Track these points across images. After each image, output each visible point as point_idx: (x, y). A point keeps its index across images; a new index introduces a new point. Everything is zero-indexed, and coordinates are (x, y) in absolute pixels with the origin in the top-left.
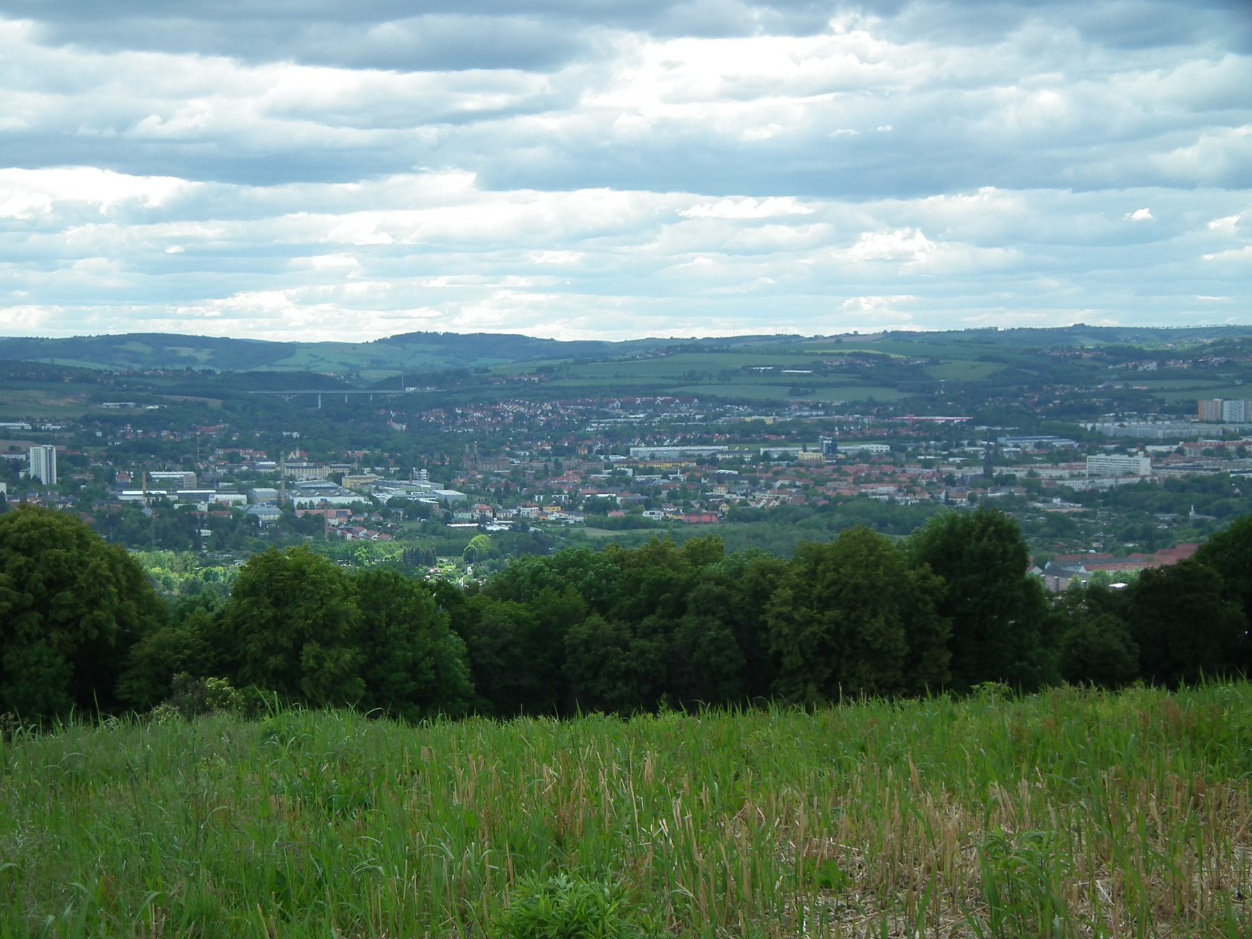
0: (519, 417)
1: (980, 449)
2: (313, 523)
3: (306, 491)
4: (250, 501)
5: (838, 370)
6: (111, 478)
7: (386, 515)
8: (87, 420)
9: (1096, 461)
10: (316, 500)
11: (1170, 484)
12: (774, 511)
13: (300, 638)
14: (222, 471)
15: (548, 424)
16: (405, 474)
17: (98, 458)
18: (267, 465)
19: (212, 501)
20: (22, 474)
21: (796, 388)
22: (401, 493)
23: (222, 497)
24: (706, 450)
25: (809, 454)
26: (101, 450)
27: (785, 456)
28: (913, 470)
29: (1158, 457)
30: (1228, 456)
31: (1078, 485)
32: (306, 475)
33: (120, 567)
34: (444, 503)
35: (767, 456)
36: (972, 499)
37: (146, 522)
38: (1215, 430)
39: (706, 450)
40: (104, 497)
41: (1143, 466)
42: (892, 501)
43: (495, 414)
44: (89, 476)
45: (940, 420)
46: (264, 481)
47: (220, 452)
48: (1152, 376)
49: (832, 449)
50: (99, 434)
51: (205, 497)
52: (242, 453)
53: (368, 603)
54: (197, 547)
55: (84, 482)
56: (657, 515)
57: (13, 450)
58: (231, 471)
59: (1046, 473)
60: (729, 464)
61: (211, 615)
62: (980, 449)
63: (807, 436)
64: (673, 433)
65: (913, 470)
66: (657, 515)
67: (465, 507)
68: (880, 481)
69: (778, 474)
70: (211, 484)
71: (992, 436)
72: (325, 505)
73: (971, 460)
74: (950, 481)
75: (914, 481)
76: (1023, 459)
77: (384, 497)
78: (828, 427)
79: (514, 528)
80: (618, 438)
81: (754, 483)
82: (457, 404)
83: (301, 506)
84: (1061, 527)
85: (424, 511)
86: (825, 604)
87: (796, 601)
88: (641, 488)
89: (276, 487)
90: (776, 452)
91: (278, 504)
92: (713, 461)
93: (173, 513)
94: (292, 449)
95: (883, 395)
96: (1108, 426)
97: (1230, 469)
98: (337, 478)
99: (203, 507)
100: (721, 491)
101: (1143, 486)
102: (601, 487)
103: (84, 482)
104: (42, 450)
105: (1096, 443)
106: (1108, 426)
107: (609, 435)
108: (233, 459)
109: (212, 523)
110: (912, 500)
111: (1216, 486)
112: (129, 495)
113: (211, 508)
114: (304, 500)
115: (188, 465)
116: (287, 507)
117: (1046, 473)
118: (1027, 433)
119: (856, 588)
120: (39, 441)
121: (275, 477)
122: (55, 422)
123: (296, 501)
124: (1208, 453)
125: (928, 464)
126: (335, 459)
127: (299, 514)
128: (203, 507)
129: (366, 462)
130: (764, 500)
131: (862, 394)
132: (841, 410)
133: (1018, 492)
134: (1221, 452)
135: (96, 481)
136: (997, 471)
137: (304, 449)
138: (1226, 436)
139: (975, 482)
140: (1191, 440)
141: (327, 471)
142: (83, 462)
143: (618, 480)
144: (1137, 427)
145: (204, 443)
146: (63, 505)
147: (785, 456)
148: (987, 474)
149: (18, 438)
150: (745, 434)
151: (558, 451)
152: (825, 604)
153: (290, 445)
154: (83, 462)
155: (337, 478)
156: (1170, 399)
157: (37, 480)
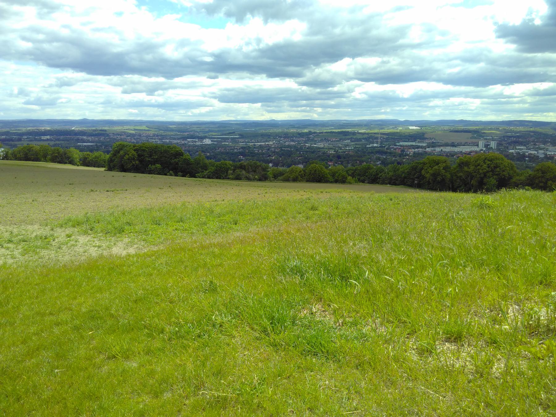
3: (550, 151)
4: (537, 153)
8: (504, 137)
14: (532, 147)
17: (505, 144)
19: (529, 153)
20: (489, 147)
23: (531, 152)
26: (505, 142)
32: (551, 148)
40: (506, 151)
44: (503, 147)
46: (541, 149)
47: (532, 143)
50: (506, 139)
51: (528, 152)
52: (537, 143)
54: (525, 161)
55: (502, 148)
57: (487, 142)
58: (534, 147)
61: (528, 175)
70: (530, 149)
83: (549, 154)
89: (544, 150)
91: (544, 154)
93: (520, 155)
94: (549, 143)
103: (502, 148)
104: (493, 142)
108: (535, 144)
112: (511, 151)
113: (529, 154)
114: (550, 153)
115: (525, 145)
116: (546, 155)
120: (493, 140)
122: (497, 137)
123: (548, 153)
127: (548, 156)
128: (527, 154)
135: (504, 148)
137: (551, 143)
142: (501, 145)
145: (529, 141)
146: (497, 154)
149: (489, 140)
153: (548, 142)
154: (501, 145)
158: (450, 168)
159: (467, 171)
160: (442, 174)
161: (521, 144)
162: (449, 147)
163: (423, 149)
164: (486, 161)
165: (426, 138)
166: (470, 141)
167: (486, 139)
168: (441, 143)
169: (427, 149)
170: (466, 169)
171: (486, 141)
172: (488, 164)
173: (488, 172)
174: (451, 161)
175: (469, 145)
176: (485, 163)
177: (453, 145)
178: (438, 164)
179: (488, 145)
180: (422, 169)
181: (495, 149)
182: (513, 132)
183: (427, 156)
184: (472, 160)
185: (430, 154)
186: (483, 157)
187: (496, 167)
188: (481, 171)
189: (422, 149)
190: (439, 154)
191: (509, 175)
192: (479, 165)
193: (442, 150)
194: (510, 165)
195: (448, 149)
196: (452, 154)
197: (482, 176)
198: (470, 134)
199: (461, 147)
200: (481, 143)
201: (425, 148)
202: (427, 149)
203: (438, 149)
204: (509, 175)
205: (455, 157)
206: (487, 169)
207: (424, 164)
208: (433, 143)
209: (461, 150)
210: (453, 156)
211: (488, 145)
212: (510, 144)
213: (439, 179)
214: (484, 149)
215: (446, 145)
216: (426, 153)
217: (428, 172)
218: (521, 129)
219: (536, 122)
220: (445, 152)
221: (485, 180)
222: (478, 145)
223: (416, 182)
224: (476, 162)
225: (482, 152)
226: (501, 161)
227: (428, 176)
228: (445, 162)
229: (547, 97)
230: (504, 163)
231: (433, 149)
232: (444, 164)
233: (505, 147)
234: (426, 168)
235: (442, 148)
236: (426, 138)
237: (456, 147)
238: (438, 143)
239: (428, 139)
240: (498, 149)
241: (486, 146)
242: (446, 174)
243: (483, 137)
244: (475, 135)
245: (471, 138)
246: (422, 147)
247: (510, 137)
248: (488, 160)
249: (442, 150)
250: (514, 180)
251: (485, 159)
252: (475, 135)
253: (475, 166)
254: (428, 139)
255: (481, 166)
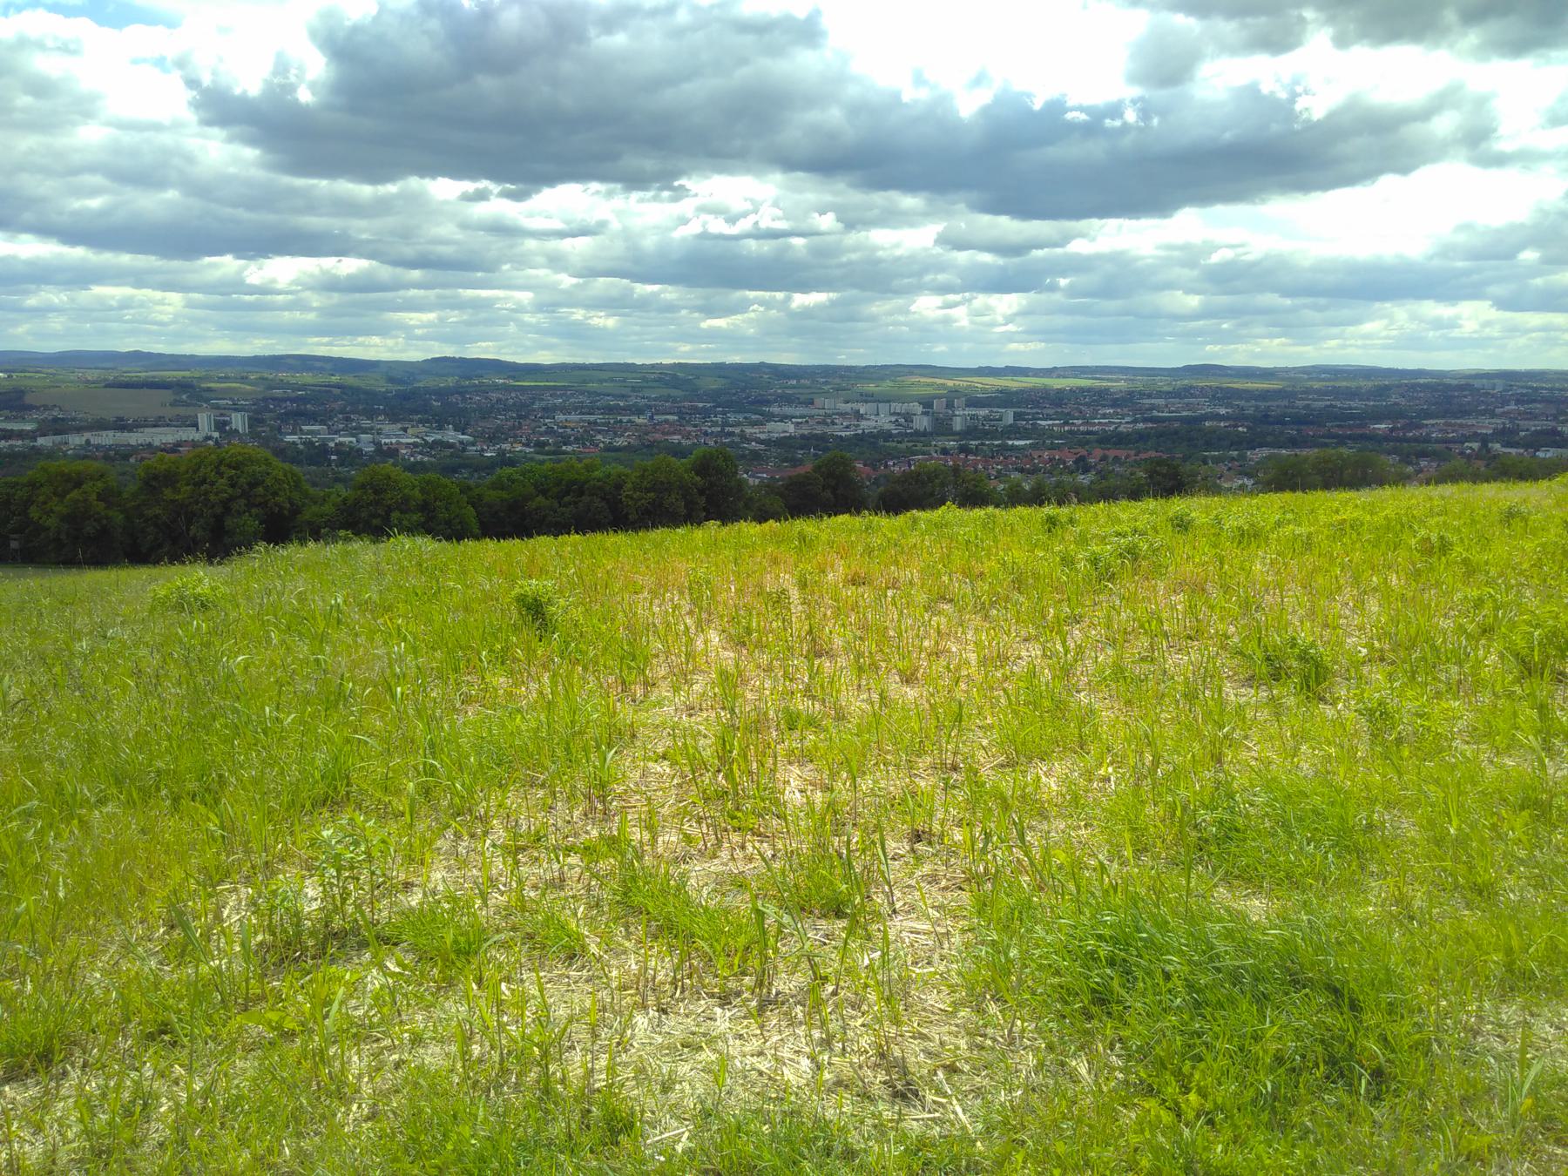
0: (499, 400)
1: (719, 419)
2: (392, 452)
3: (388, 436)
5: (655, 380)
6: (279, 429)
7: (431, 448)
8: (265, 399)
9: (770, 426)
10: (394, 441)
11: (803, 436)
12: (625, 447)
13: (389, 510)
14: (341, 426)
15: (514, 404)
16: (440, 428)
18: (366, 423)
21: (634, 389)
22: (439, 437)
24: (592, 418)
25: (640, 420)
27: (630, 421)
28: (689, 428)
29: (798, 424)
30: (827, 424)
31: (763, 436)
32: (388, 428)
33: (289, 475)
34: (461, 442)
35: (621, 421)
36: (716, 442)
37: (300, 452)
38: (822, 412)
39: (592, 418)
40: (276, 439)
41: (791, 428)
42: (680, 443)
43: (486, 398)
45: (701, 405)
48: (794, 387)
49: (652, 418)
51: (333, 439)
53: (422, 491)
56: (569, 448)
57: (222, 415)
59: (749, 430)
60: (603, 424)
62: (719, 419)
63: (639, 412)
64: (576, 409)
65: (689, 428)
66: (569, 448)
67: (473, 444)
68: (674, 433)
69: (626, 430)
70: (336, 432)
71: (724, 413)
72: (398, 443)
73: (715, 424)
74: (706, 434)
75: (689, 433)
76: (738, 424)
77: (430, 439)
78: (650, 407)
79: (498, 455)
80: (549, 411)
81: (615, 433)
82: (466, 392)
84: (756, 456)
85: (451, 446)
86: (648, 490)
87: (635, 489)
88: (561, 435)
90: (625, 419)
91: (373, 442)
92: (595, 423)
95: (674, 392)
96: (775, 409)
97: (828, 430)
98: (405, 430)
99: (332, 444)
100: (599, 437)
101: (790, 437)
102: (542, 434)
104: (239, 415)
105: (770, 417)
106: (775, 409)
107: (544, 409)
108: (348, 419)
109: (337, 452)
110: (689, 442)
111: (823, 438)
112: (289, 438)
114: (387, 441)
115: (322, 423)
116: (378, 444)
117: (749, 430)
118: (739, 412)
119: (662, 483)
120: (236, 410)
121: (372, 429)
124: (818, 423)
125: (695, 426)
126: (404, 420)
128: (332, 444)
129: (420, 421)
130: (620, 442)
131: (665, 392)
132: (655, 399)
133: (737, 439)
134: (824, 423)
136: (727, 429)
137: (387, 415)
138: (827, 415)
139: (718, 435)
140: (812, 417)
141: (399, 426)
142: (261, 422)
143: (550, 431)
144: (788, 410)
147: (630, 421)
148: (723, 430)
150: (610, 410)
151: (520, 417)
152: (648, 490)
153: (378, 413)
154: (261, 422)
155: (405, 430)
156: (802, 398)
157: (236, 431)
158: (120, 494)
159: (173, 501)
160: (98, 513)
161: (313, 418)
162: (111, 433)
163: (27, 442)
164: (223, 468)
165: (30, 408)
166: (169, 412)
167: (217, 407)
168: (81, 420)
169: (41, 441)
170: (168, 493)
171: (218, 412)
172: (231, 478)
173: (232, 499)
174: (124, 474)
175: (168, 425)
176: (221, 475)
177: (121, 425)
178: (78, 484)
179: (225, 423)
180: (28, 502)
181: (245, 434)
182: (288, 385)
183: (41, 464)
184: (183, 469)
185: (51, 454)
186: (213, 456)
187: (253, 485)
188: (212, 497)
189: (23, 440)
190: (82, 452)
191: (292, 504)
192: (204, 481)
193: (88, 442)
194: (289, 475)
195: (107, 438)
196: (124, 454)
197: (219, 510)
198: (170, 391)
199: (147, 430)
200: (204, 419)
201: (32, 436)
202: (41, 441)
203: (76, 440)
204: (292, 504)
205: (132, 460)
206: (230, 491)
207: (33, 485)
208: (56, 420)
209: (149, 440)
210: (126, 457)
211: (225, 423)
212: (287, 417)
213: (89, 528)
214: (216, 435)
215: (101, 425)
216: (37, 452)
217: (52, 511)
218: (307, 378)
219: (340, 360)
220: (98, 447)
221: (229, 522)
222: (195, 425)
223: (14, 545)
224: (195, 472)
225: (210, 442)
226: (264, 467)
227: (51, 522)
228: (102, 476)
229: (357, 296)
230: (275, 472)
231: (58, 438)
232: (100, 484)
233: (272, 428)
234: (41, 498)
235: (87, 435)
236: (30, 408)
237: (130, 431)
238: (74, 419)
239: (37, 408)
240: (254, 435)
241: (221, 426)
242: (111, 513)
243: (207, 400)
244: (184, 397)
245: (174, 404)
246: (21, 435)
247: (285, 400)
248: (229, 466)
249: (88, 442)
250: (307, 515)
251: (221, 462)
252: (184, 397)
253: (194, 485)
254: (37, 408)
255: (212, 484)
